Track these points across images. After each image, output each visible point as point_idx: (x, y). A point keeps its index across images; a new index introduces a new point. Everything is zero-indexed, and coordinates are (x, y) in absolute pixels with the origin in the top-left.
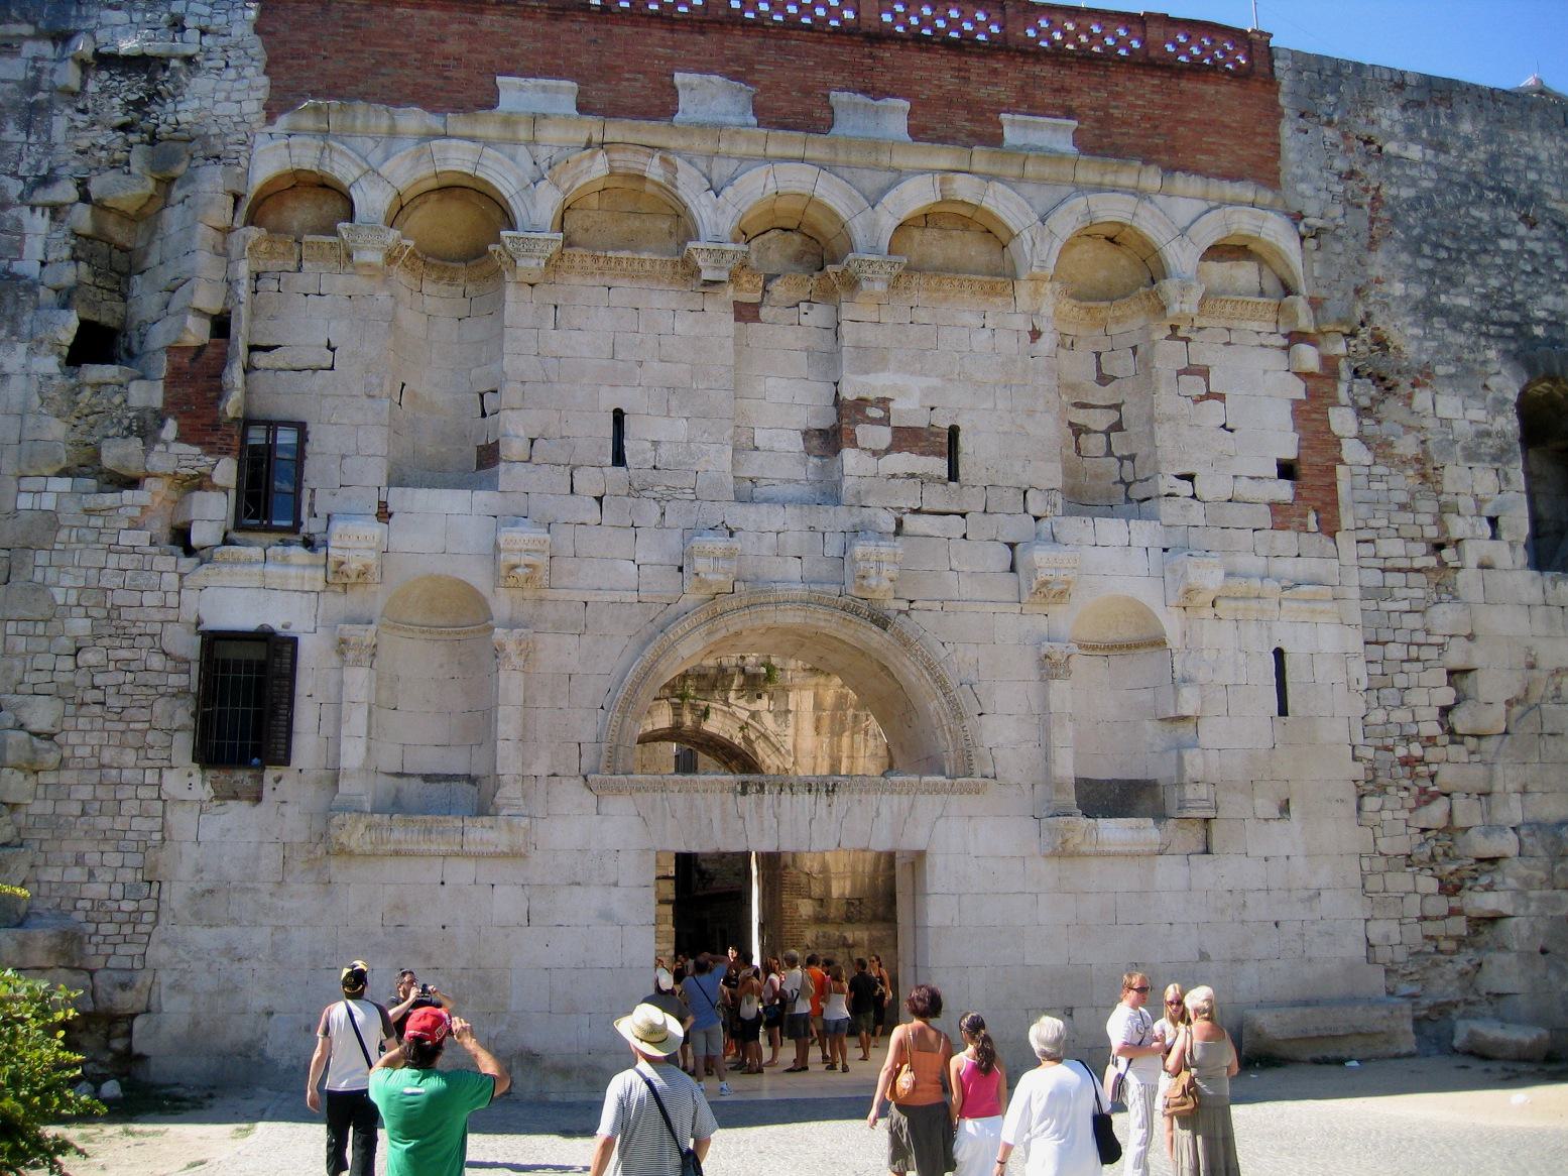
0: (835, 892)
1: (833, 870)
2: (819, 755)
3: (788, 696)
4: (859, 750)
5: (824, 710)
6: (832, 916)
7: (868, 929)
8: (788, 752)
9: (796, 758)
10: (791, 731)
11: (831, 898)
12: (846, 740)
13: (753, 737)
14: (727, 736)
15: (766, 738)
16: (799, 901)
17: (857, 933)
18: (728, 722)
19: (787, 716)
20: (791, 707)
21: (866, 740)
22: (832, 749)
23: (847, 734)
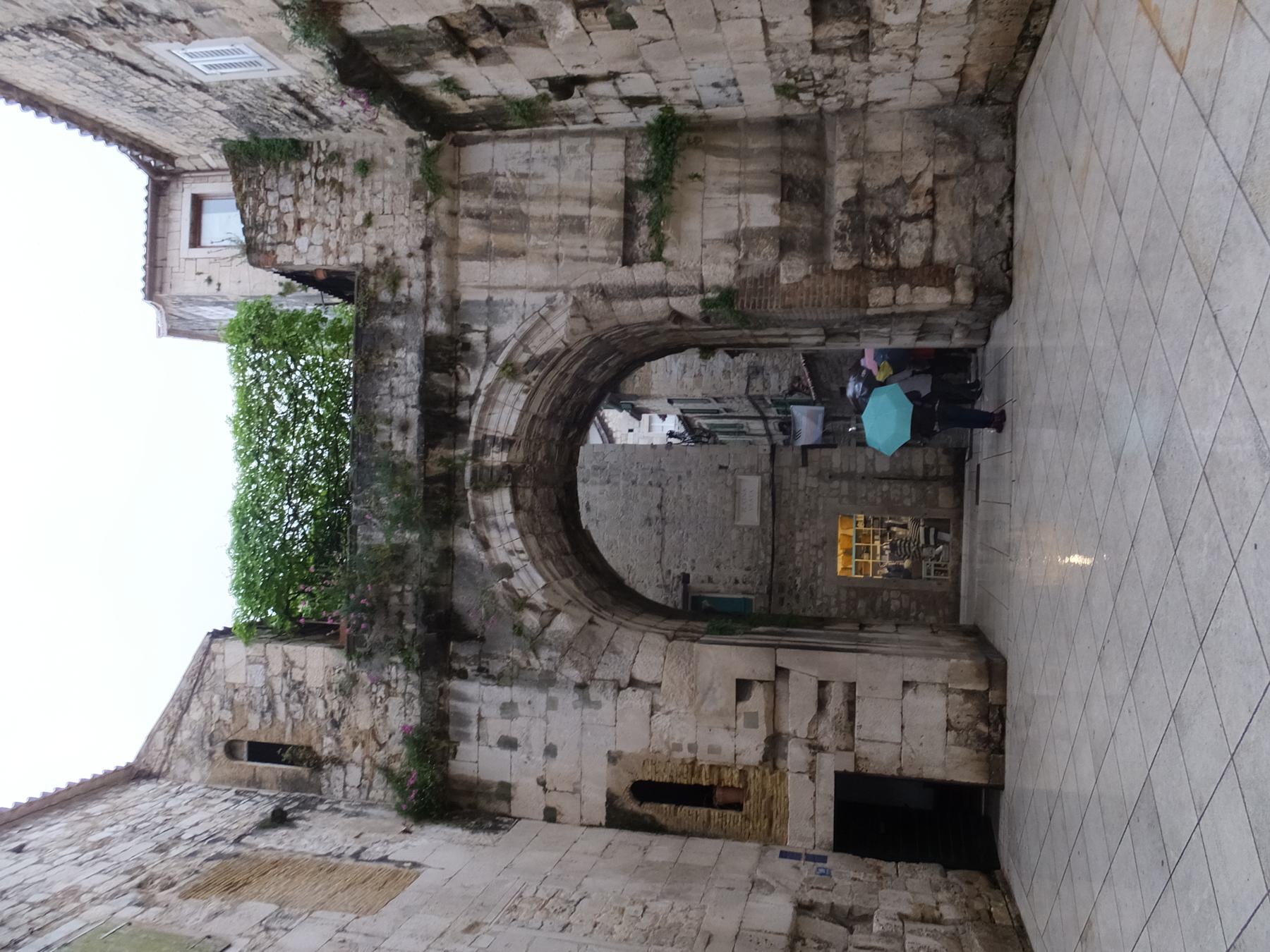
0: (774, 221)
1: (734, 225)
2: (552, 251)
3: (467, 303)
4: (548, 188)
5: (489, 244)
6: (809, 225)
7: (832, 166)
8: (549, 301)
9: (557, 289)
10: (518, 296)
11: (779, 228)
12: (535, 209)
13: (524, 358)
14: (524, 397)
15: (526, 336)
16: (784, 281)
17: (837, 183)
18: (502, 397)
19: (496, 304)
20: (482, 296)
21: (535, 176)
22: (545, 231)
23: (523, 207)
